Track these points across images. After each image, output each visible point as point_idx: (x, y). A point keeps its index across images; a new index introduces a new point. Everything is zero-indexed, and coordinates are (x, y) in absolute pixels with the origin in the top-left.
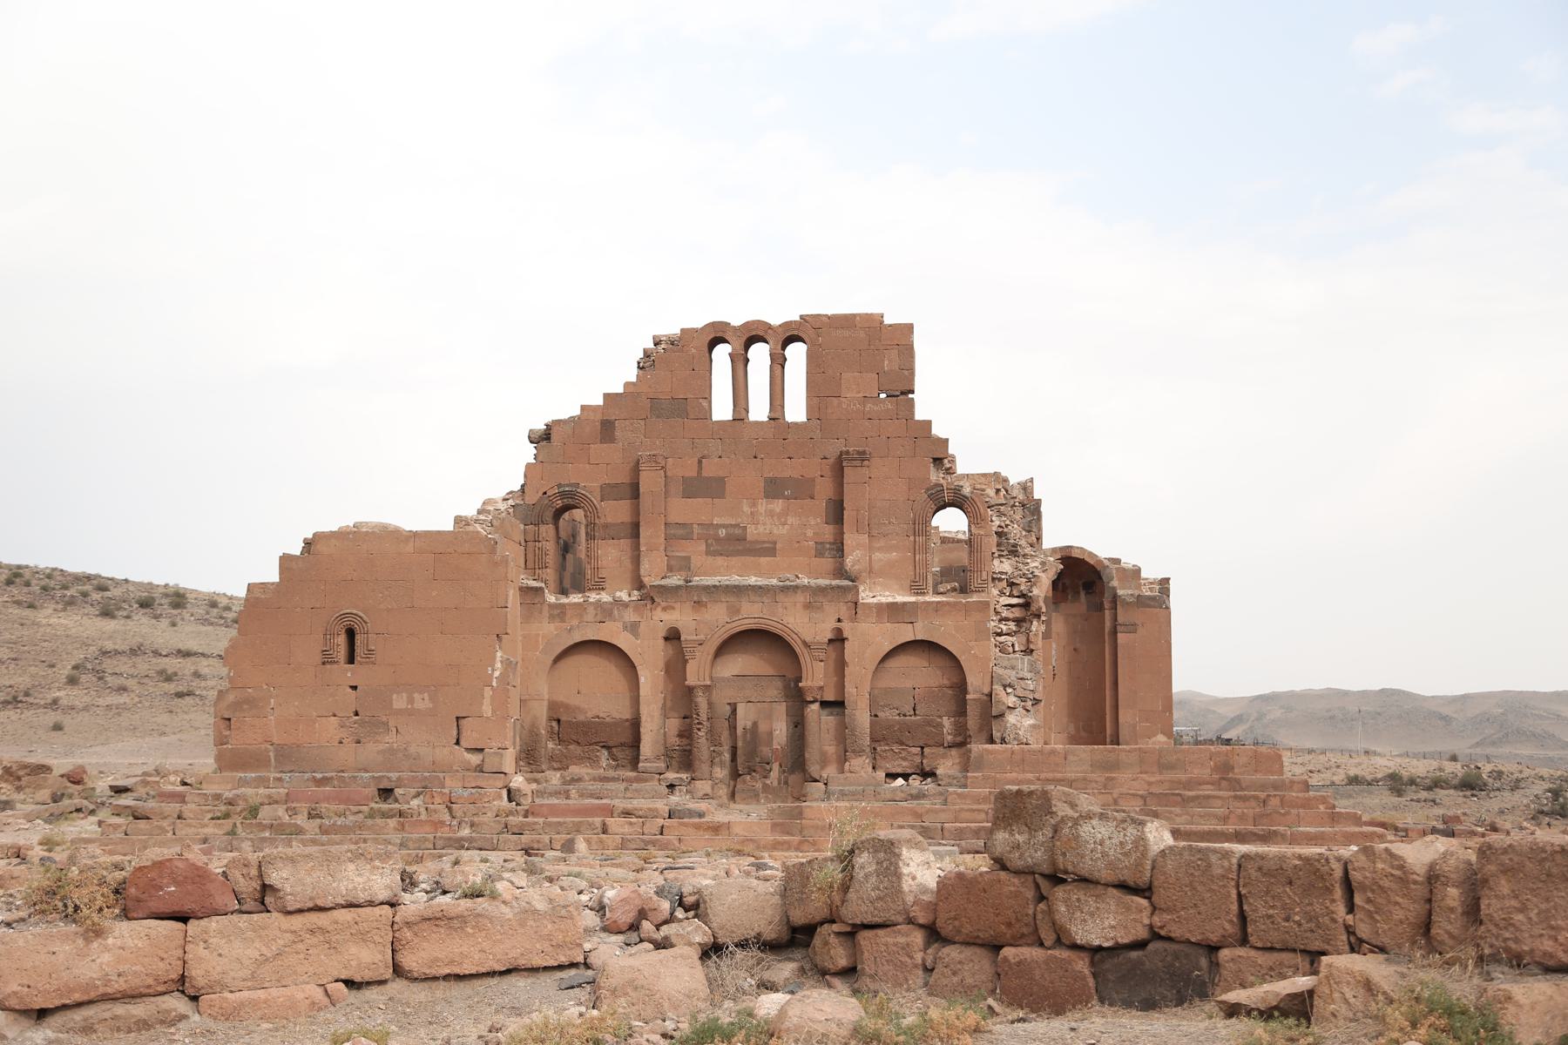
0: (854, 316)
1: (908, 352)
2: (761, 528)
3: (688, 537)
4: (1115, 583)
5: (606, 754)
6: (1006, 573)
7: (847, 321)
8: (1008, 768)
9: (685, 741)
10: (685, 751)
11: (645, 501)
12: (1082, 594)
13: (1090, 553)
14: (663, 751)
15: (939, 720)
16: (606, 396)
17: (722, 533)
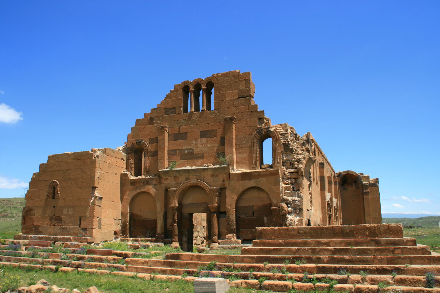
0: (230, 72)
4: (362, 181)
5: (149, 231)
6: (290, 160)
7: (226, 75)
8: (273, 237)
12: (354, 184)
13: (355, 173)
16: (152, 110)
17: (186, 152)
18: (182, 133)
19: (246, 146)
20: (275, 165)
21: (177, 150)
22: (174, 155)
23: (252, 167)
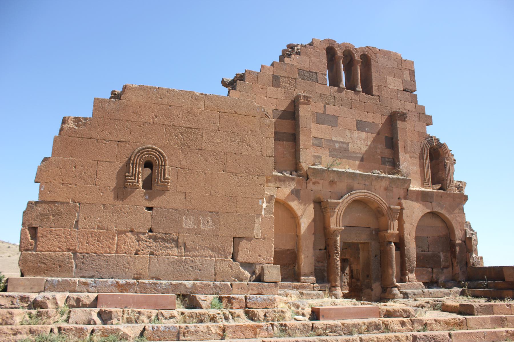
1: (412, 73)
2: (356, 147)
3: (319, 146)
9: (321, 264)
10: (320, 270)
11: (302, 121)
14: (314, 271)
15: (439, 254)
17: (337, 145)
18: (327, 114)
19: (416, 156)
20: (449, 188)
21: (323, 140)
22: (319, 147)
23: (425, 185)
